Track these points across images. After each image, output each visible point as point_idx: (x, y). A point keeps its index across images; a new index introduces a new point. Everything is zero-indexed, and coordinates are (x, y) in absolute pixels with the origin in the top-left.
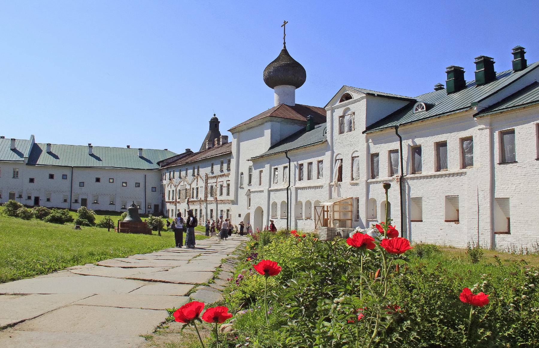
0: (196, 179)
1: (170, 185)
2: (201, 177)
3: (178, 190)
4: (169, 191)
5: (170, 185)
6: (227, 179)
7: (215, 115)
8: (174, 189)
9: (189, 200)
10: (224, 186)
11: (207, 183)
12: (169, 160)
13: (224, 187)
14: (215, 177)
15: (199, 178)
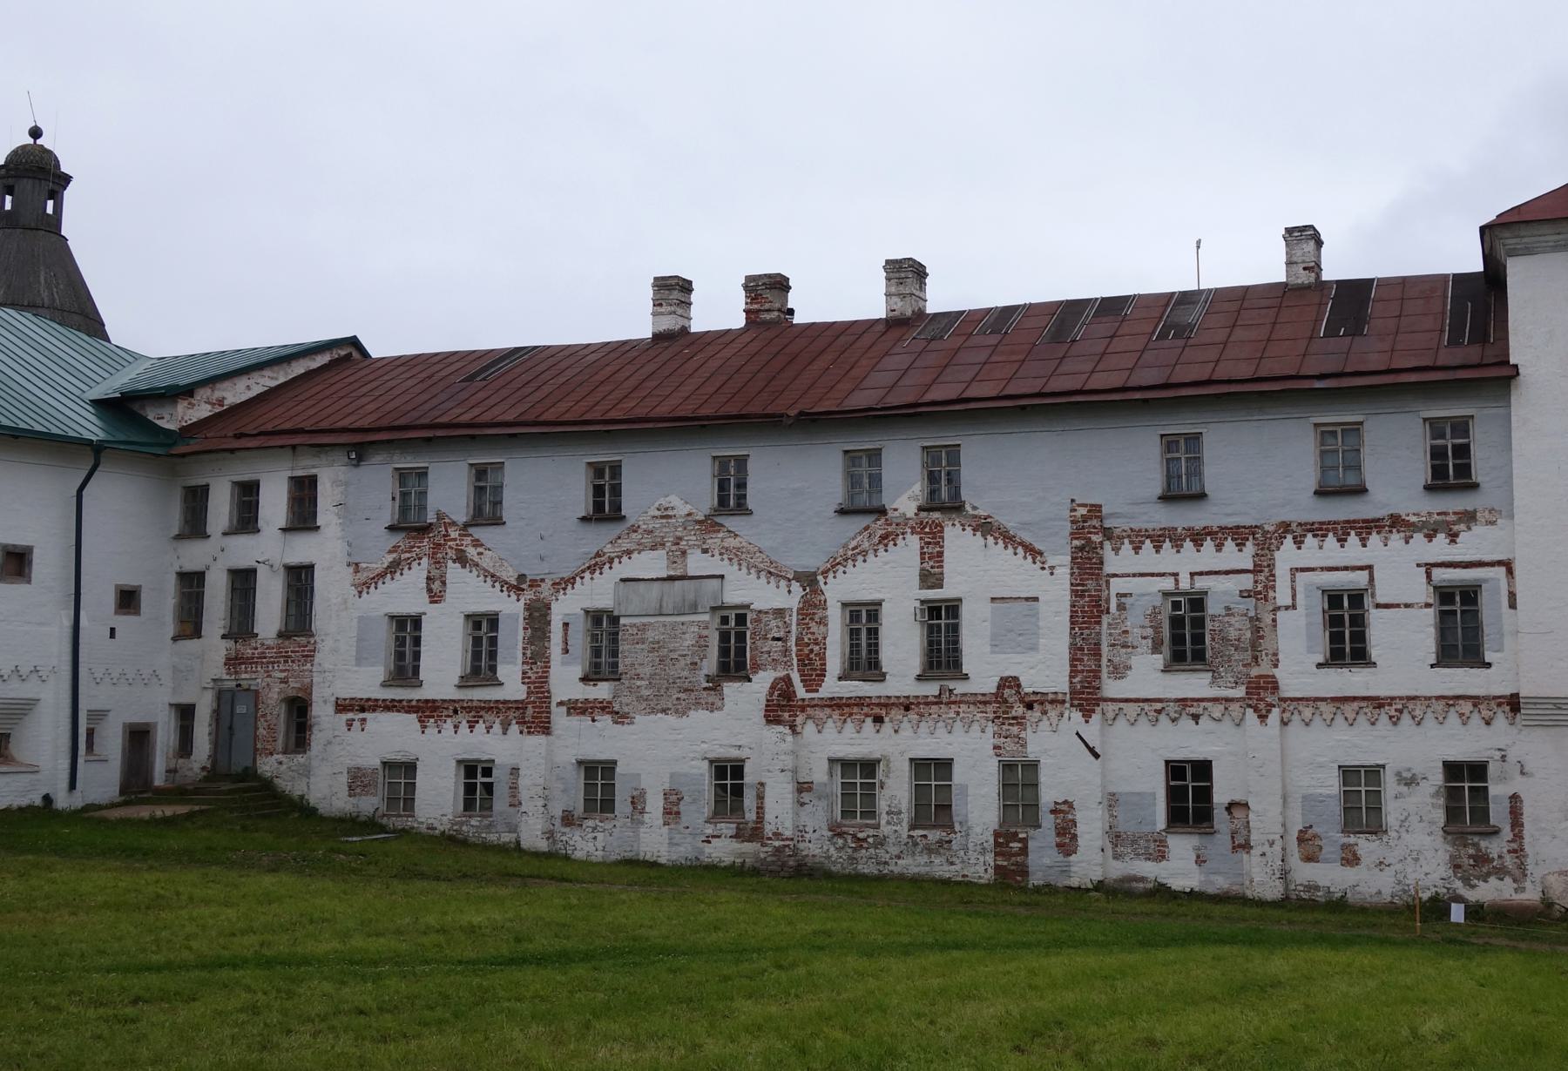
0: (914, 542)
1: (416, 576)
2: (985, 527)
3: (567, 607)
4: (407, 629)
5: (416, 576)
6: (1440, 549)
7: (36, 133)
8: (511, 608)
9: (801, 692)
10: (1380, 600)
11: (1087, 565)
12: (227, 384)
13: (1378, 606)
14: (1240, 535)
15: (959, 542)
